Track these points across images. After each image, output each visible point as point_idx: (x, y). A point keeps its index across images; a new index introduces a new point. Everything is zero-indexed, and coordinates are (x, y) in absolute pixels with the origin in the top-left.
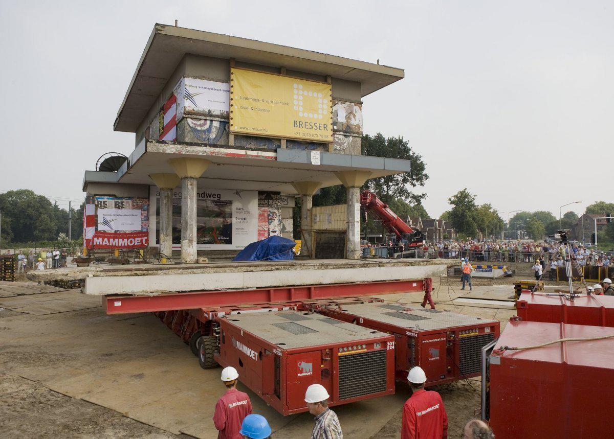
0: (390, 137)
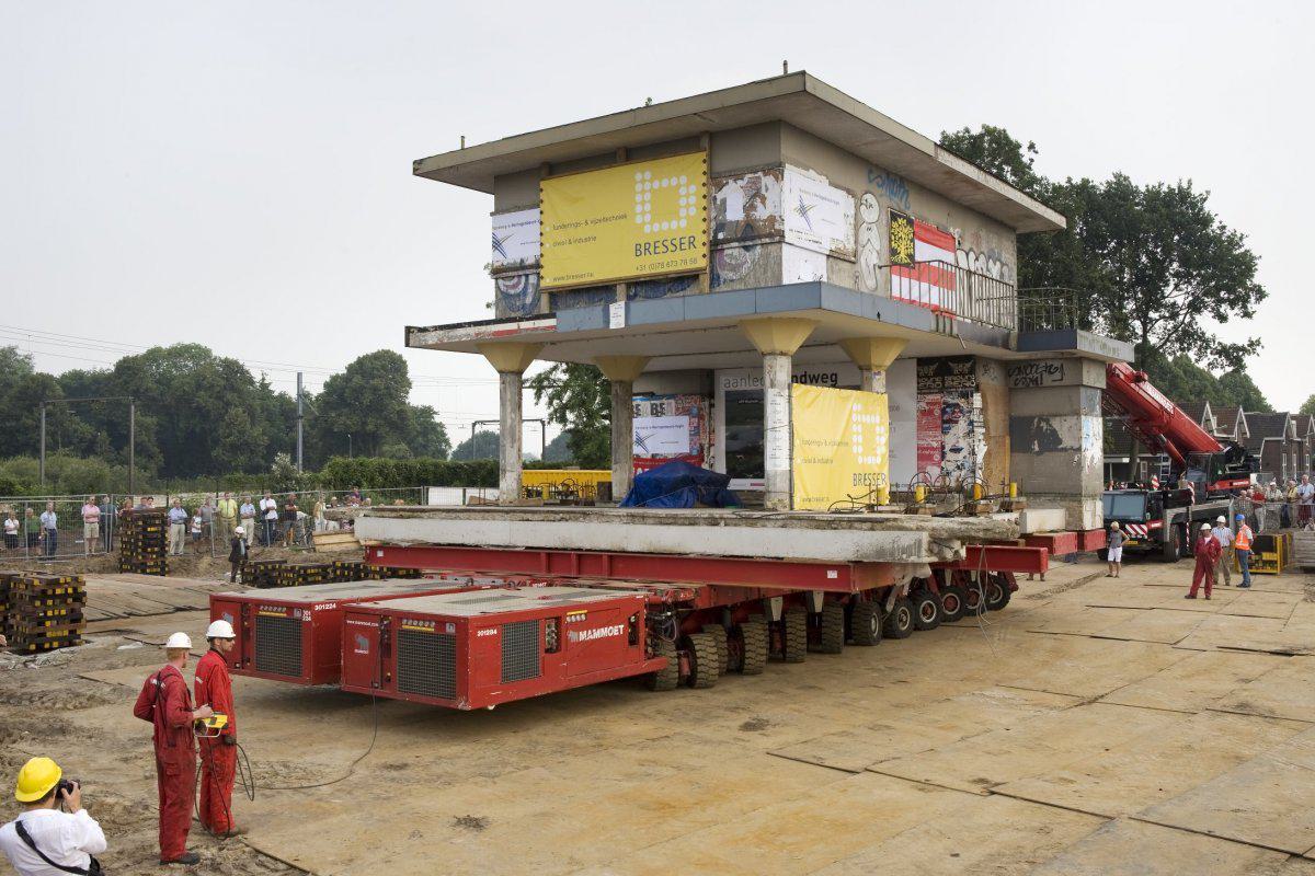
0: (1153, 183)
